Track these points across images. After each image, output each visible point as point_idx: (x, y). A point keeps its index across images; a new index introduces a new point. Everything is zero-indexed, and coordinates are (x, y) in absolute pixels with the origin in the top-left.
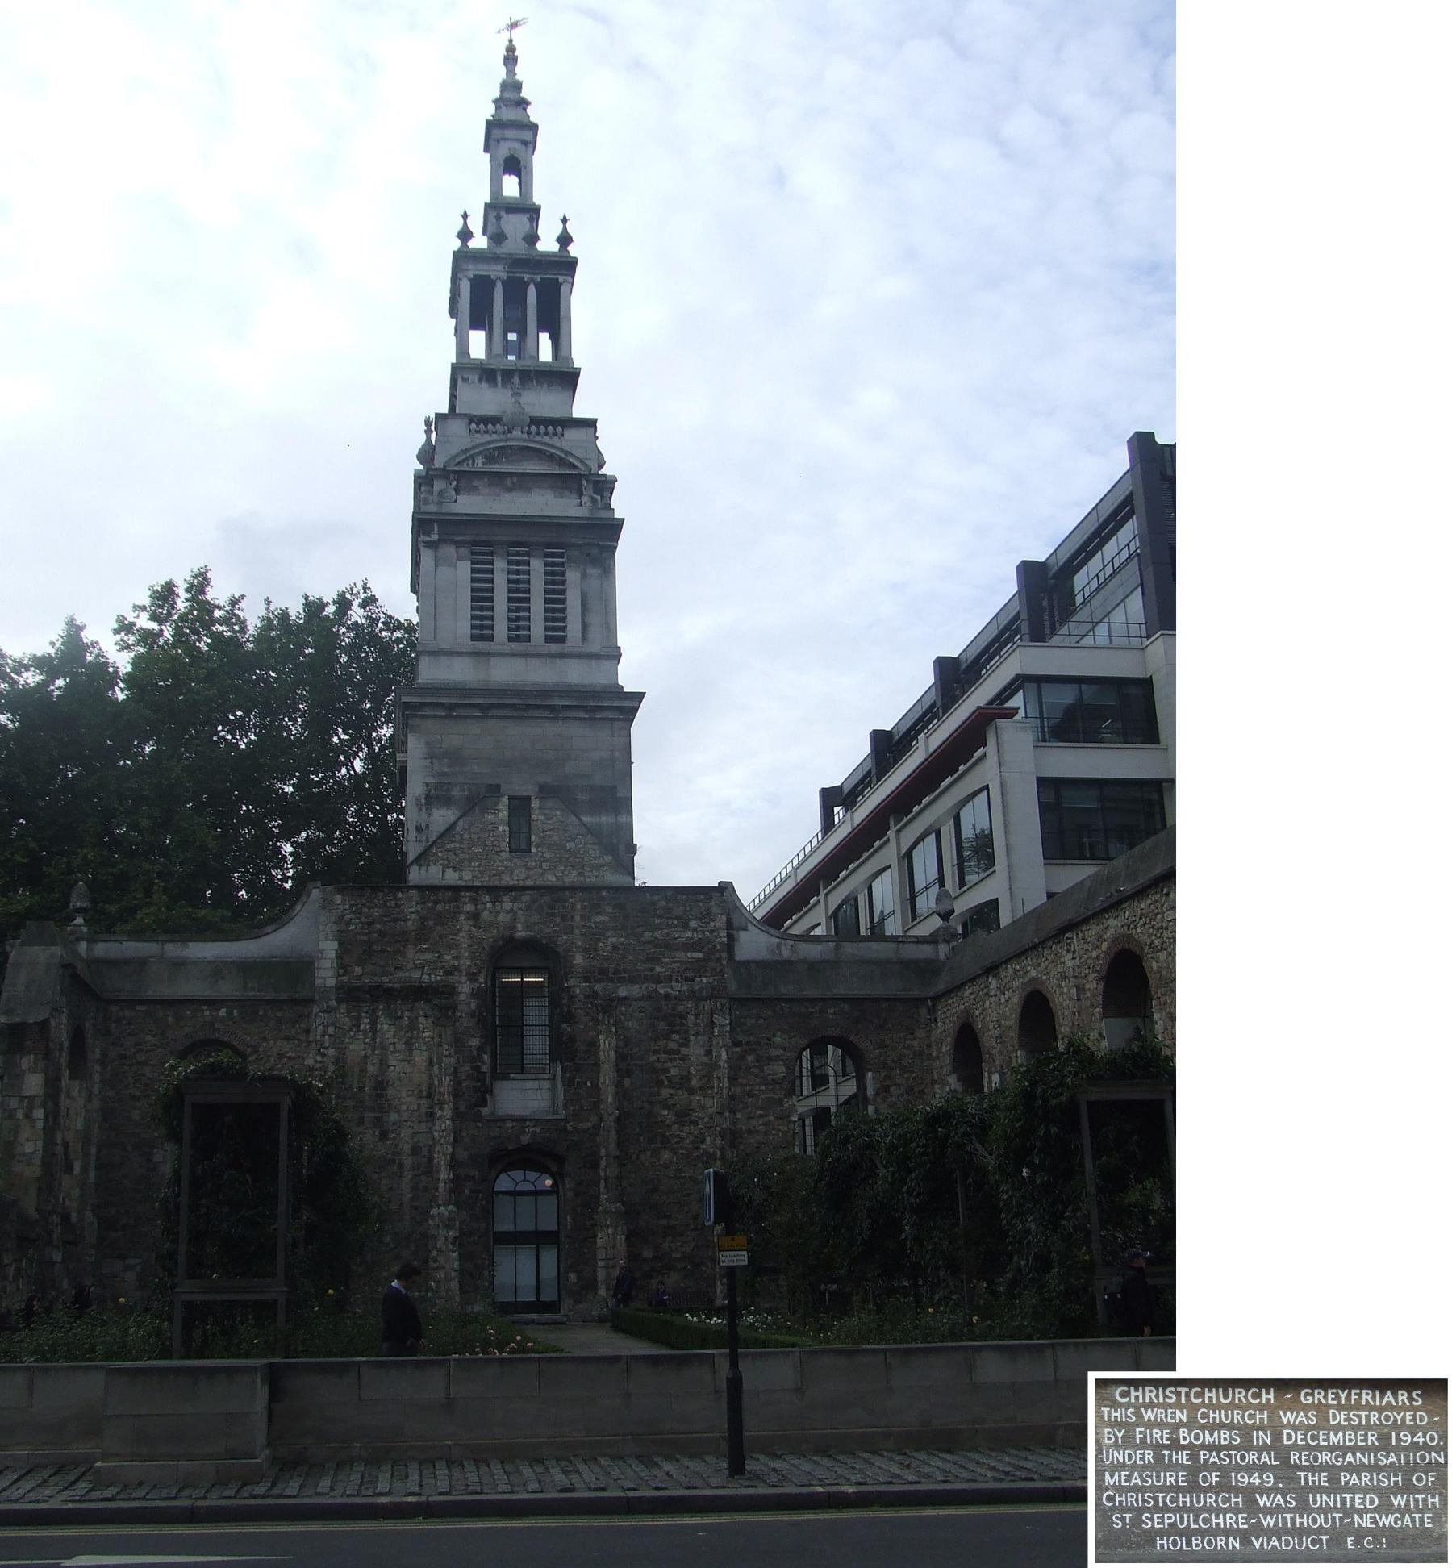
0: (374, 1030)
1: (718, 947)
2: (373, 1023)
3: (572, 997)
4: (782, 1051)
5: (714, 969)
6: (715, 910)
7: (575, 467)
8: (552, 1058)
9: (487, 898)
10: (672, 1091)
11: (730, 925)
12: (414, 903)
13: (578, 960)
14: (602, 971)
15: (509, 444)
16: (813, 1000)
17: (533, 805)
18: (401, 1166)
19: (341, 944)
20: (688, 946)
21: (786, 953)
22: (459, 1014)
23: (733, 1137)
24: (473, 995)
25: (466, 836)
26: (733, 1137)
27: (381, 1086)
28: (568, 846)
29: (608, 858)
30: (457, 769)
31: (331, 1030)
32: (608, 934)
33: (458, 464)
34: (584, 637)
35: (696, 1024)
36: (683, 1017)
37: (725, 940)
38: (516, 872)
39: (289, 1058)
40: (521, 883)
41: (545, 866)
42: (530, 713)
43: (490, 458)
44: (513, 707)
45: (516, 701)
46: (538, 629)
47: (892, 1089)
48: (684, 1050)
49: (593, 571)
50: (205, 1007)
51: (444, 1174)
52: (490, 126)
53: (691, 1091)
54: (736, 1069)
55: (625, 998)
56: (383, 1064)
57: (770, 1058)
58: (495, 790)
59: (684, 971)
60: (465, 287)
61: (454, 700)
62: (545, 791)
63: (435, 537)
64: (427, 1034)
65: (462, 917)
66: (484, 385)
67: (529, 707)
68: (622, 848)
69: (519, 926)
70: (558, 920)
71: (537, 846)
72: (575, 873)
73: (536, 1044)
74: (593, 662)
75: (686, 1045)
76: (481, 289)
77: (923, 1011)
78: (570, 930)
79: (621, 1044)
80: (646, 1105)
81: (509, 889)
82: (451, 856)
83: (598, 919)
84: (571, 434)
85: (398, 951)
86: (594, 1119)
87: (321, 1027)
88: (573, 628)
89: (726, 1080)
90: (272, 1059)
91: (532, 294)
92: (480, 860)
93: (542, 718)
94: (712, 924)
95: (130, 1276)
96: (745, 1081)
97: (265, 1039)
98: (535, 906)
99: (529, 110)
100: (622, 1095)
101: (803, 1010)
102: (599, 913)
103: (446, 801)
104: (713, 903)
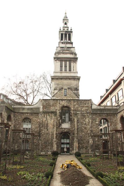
2: (47, 116)
8: (69, 121)
11: (91, 104)
13: (72, 108)
14: (75, 110)
16: (102, 114)
20: (86, 107)
21: (98, 108)
23: (92, 131)
26: (92, 131)
27: (47, 124)
29: (76, 96)
43: (63, 51)
44: (65, 78)
49: (74, 63)
51: (55, 135)
52: (63, 19)
54: (92, 122)
56: (48, 121)
57: (96, 121)
58: (62, 88)
60: (60, 34)
63: (56, 60)
76: (62, 35)
77: (116, 115)
81: (64, 100)
84: (72, 49)
86: (74, 129)
91: (68, 35)
95: (16, 146)
100: (78, 126)
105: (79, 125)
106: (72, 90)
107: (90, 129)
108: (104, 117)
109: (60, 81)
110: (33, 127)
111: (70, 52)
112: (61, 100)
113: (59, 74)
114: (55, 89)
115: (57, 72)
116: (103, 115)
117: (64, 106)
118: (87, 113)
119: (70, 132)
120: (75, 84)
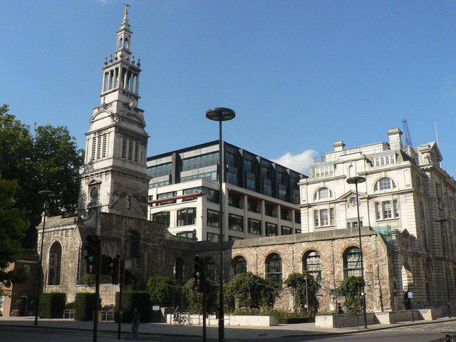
24: (125, 241)
46: (133, 158)
62: (134, 196)
103: (117, 195)
112: (129, 217)
113: (120, 164)
117: (131, 229)
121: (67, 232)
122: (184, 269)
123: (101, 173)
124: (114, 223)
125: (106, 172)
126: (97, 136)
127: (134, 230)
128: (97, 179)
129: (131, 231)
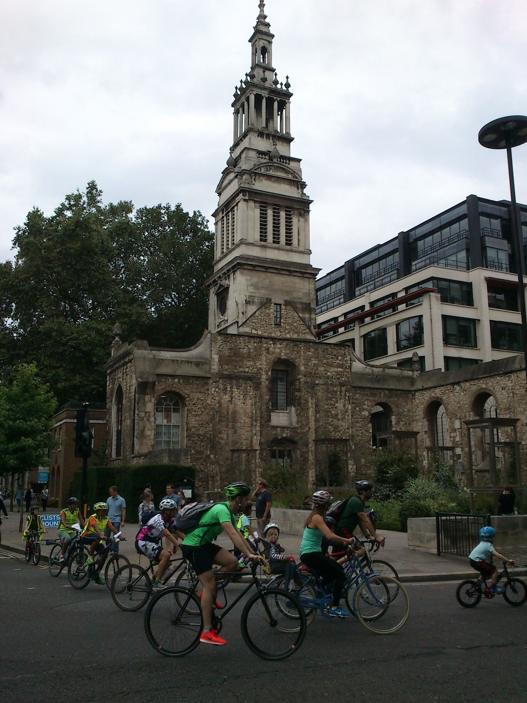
0: (232, 392)
1: (348, 367)
3: (300, 382)
4: (367, 407)
5: (346, 375)
6: (347, 353)
7: (297, 178)
9: (271, 342)
10: (332, 419)
11: (351, 361)
12: (246, 342)
13: (302, 368)
14: (310, 373)
15: (274, 164)
16: (377, 389)
17: (282, 308)
18: (241, 444)
19: (220, 357)
20: (339, 366)
22: (262, 386)
25: (259, 317)
27: (235, 412)
28: (295, 324)
29: (308, 331)
30: (257, 291)
31: (217, 390)
32: (312, 359)
33: (255, 170)
34: (298, 245)
35: (340, 395)
36: (336, 392)
37: (350, 365)
38: (277, 333)
39: (202, 400)
40: (278, 337)
41: (287, 331)
42: (282, 272)
44: (277, 269)
45: (278, 267)
47: (401, 422)
48: (336, 405)
49: (302, 220)
50: (169, 378)
53: (338, 420)
55: (318, 384)
57: (363, 409)
59: (337, 375)
61: (256, 264)
63: (247, 198)
64: (250, 393)
65: (263, 349)
66: (259, 137)
67: (282, 269)
68: (312, 327)
69: (283, 354)
70: (296, 353)
71: (284, 323)
72: (296, 335)
73: (281, 399)
74: (302, 255)
75: (337, 403)
77: (410, 395)
78: (300, 357)
79: (316, 401)
80: (324, 424)
82: (254, 325)
83: (309, 353)
84: (292, 164)
85: (240, 361)
86: (307, 428)
87: (213, 389)
88: (295, 241)
89: (350, 416)
90: (195, 400)
91: (276, 104)
92: (264, 327)
93: (285, 274)
94: (346, 358)
96: (355, 417)
97: (192, 392)
98: (288, 346)
99: (270, 28)
100: (317, 420)
101: (374, 392)
102: (309, 351)
104: (346, 351)
105: (320, 417)
106: (296, 310)
107: (347, 430)
108: (383, 400)
109: (263, 275)
110: (193, 421)
111: (290, 177)
112: (272, 339)
113: (255, 252)
114: (247, 303)
115: (252, 244)
116: (380, 393)
117: (280, 358)
118: (342, 385)
119: (296, 439)
120: (304, 291)
121: (127, 368)
122: (394, 423)
123: (228, 271)
124: (245, 351)
125: (233, 267)
126: (225, 213)
127: (284, 359)
128: (225, 282)
129: (279, 361)
